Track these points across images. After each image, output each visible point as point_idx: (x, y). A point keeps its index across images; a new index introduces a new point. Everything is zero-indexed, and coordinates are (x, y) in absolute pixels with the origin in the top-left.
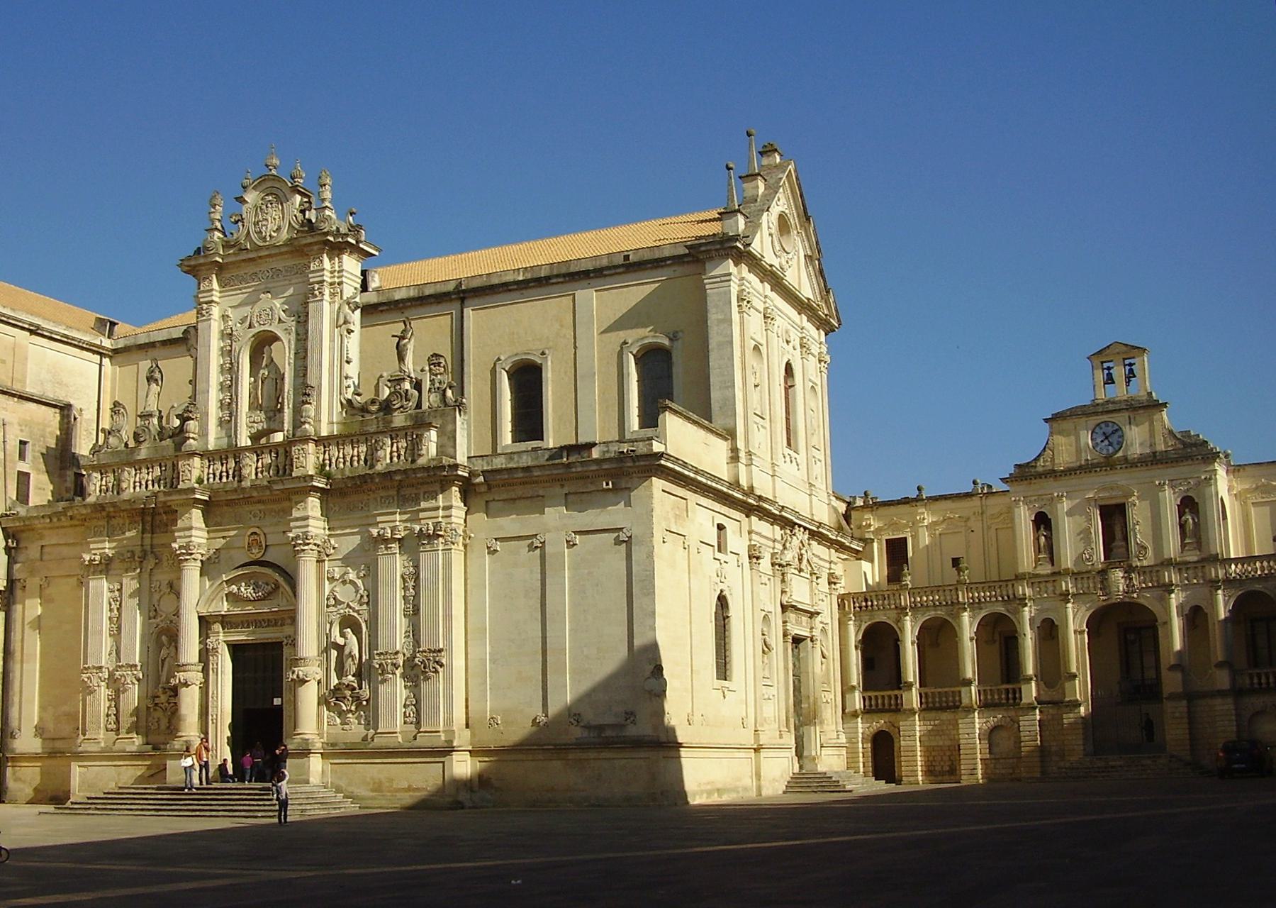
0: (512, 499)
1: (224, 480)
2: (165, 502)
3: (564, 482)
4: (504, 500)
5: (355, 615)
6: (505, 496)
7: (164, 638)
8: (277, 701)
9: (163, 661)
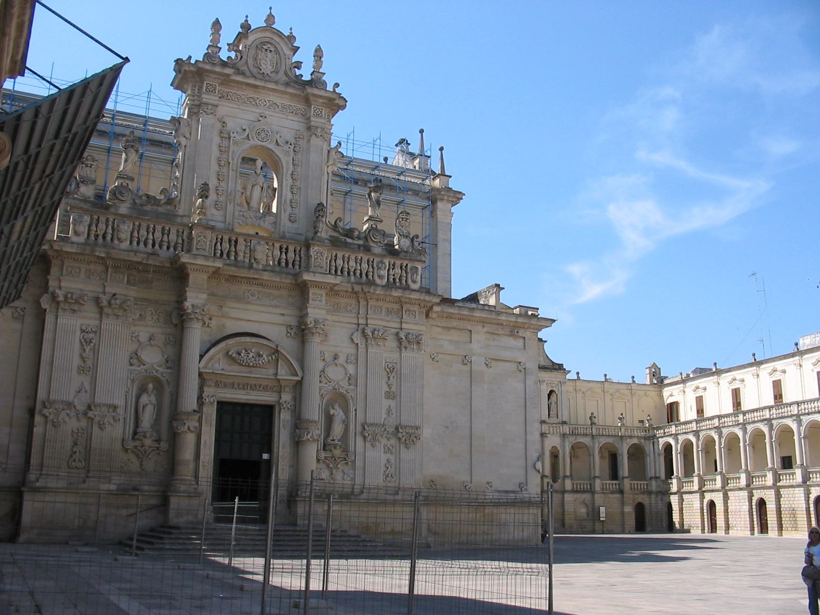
0: (448, 327)
1: (232, 258)
2: (184, 263)
3: (485, 325)
4: (443, 327)
5: (345, 392)
6: (444, 324)
7: (151, 386)
8: (265, 456)
9: (144, 407)
